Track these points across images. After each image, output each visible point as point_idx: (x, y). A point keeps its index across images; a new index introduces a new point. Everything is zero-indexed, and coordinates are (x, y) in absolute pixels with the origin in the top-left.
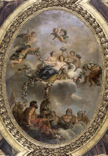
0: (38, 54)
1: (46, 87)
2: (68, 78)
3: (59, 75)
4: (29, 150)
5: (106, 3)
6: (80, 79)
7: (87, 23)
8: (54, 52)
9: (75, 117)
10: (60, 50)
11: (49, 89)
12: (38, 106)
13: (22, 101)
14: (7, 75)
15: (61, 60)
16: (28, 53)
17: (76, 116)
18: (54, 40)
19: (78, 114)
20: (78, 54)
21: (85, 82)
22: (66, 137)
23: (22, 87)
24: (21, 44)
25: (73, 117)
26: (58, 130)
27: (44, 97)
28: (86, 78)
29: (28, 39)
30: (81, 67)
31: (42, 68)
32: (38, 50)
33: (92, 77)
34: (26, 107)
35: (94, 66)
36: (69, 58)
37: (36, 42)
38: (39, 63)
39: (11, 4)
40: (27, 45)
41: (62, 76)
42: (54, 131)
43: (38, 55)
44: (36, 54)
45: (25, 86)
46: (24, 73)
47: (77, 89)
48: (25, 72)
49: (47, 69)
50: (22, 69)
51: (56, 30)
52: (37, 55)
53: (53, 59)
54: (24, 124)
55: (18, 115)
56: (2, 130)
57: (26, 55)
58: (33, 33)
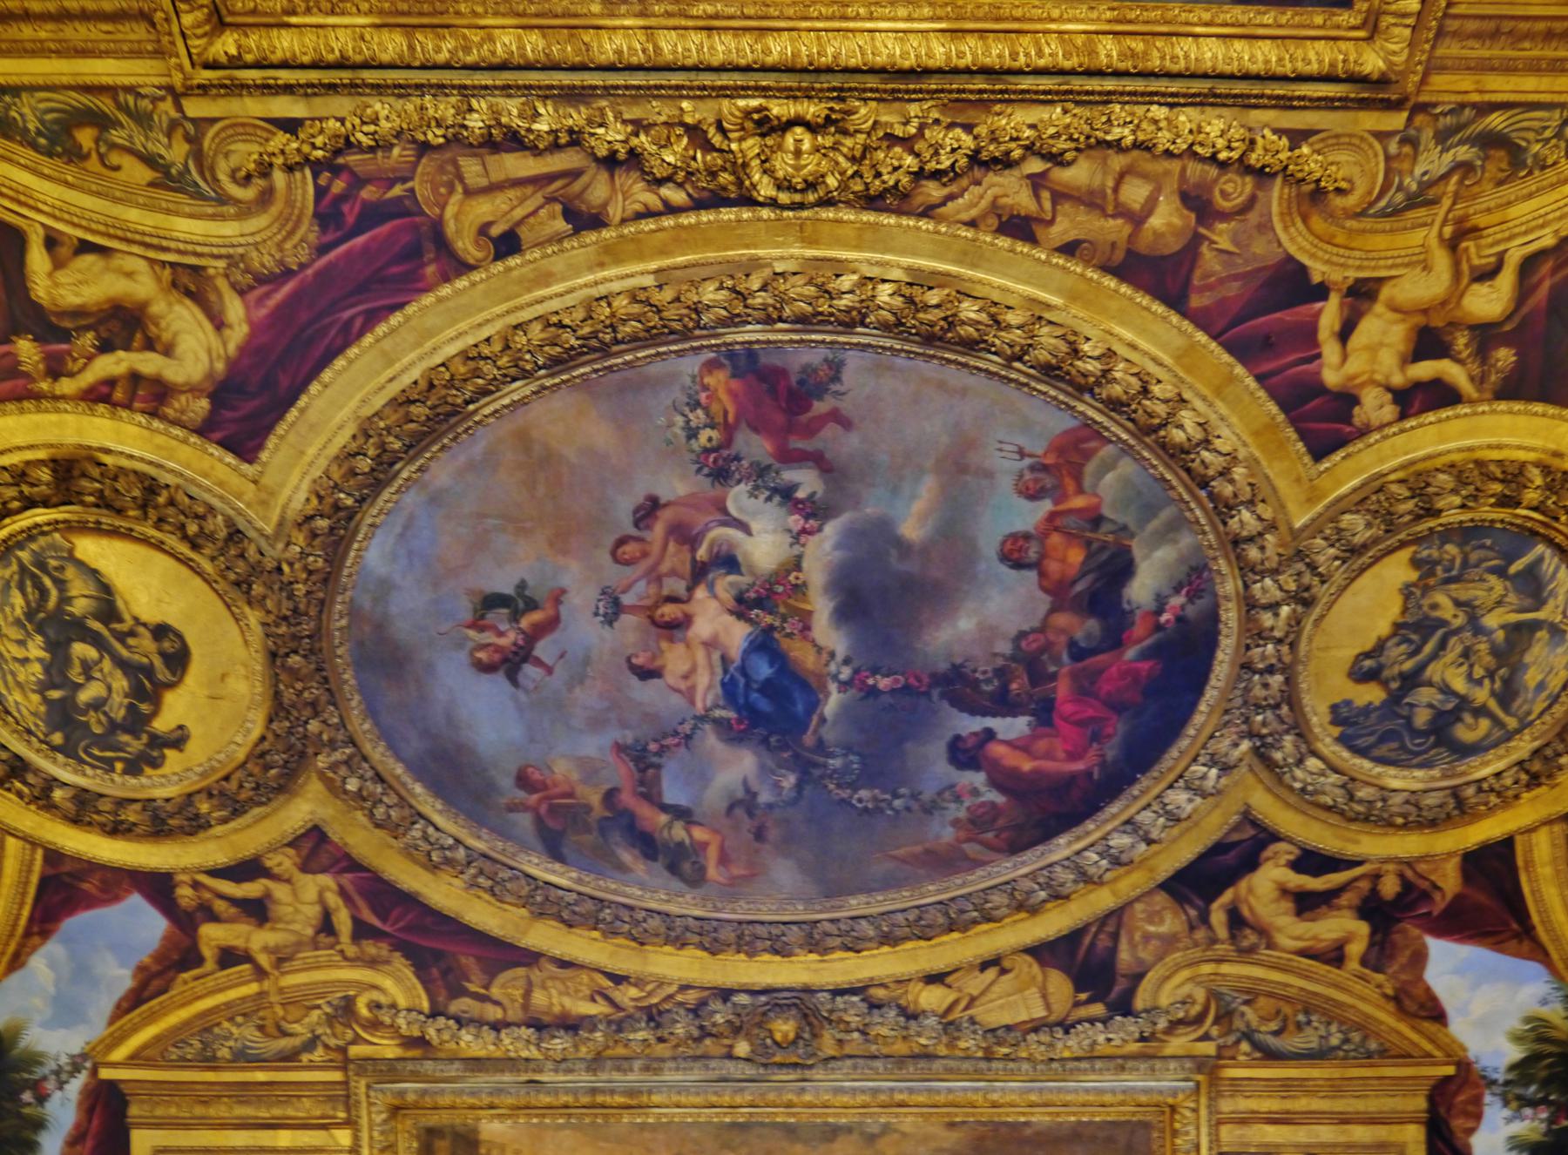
3: (777, 624)
5: (225, 344)
6: (801, 494)
7: (405, 474)
8: (634, 661)
9: (1052, 516)
10: (616, 624)
17: (1046, 506)
19: (1033, 495)
21: (818, 461)
22: (1182, 560)
25: (1056, 529)
26: (1132, 612)
27: (923, 701)
28: (789, 457)
30: (718, 490)
31: (739, 721)
33: (780, 419)
34: (983, 789)
35: (706, 410)
36: (665, 567)
38: (710, 740)
39: (361, 903)
41: (787, 605)
42: (1139, 629)
44: (655, 760)
45: (860, 800)
47: (868, 510)
48: (770, 806)
52: (659, 754)
53: (675, 660)
56: (1114, 893)
57: (665, 808)
58: (523, 780)
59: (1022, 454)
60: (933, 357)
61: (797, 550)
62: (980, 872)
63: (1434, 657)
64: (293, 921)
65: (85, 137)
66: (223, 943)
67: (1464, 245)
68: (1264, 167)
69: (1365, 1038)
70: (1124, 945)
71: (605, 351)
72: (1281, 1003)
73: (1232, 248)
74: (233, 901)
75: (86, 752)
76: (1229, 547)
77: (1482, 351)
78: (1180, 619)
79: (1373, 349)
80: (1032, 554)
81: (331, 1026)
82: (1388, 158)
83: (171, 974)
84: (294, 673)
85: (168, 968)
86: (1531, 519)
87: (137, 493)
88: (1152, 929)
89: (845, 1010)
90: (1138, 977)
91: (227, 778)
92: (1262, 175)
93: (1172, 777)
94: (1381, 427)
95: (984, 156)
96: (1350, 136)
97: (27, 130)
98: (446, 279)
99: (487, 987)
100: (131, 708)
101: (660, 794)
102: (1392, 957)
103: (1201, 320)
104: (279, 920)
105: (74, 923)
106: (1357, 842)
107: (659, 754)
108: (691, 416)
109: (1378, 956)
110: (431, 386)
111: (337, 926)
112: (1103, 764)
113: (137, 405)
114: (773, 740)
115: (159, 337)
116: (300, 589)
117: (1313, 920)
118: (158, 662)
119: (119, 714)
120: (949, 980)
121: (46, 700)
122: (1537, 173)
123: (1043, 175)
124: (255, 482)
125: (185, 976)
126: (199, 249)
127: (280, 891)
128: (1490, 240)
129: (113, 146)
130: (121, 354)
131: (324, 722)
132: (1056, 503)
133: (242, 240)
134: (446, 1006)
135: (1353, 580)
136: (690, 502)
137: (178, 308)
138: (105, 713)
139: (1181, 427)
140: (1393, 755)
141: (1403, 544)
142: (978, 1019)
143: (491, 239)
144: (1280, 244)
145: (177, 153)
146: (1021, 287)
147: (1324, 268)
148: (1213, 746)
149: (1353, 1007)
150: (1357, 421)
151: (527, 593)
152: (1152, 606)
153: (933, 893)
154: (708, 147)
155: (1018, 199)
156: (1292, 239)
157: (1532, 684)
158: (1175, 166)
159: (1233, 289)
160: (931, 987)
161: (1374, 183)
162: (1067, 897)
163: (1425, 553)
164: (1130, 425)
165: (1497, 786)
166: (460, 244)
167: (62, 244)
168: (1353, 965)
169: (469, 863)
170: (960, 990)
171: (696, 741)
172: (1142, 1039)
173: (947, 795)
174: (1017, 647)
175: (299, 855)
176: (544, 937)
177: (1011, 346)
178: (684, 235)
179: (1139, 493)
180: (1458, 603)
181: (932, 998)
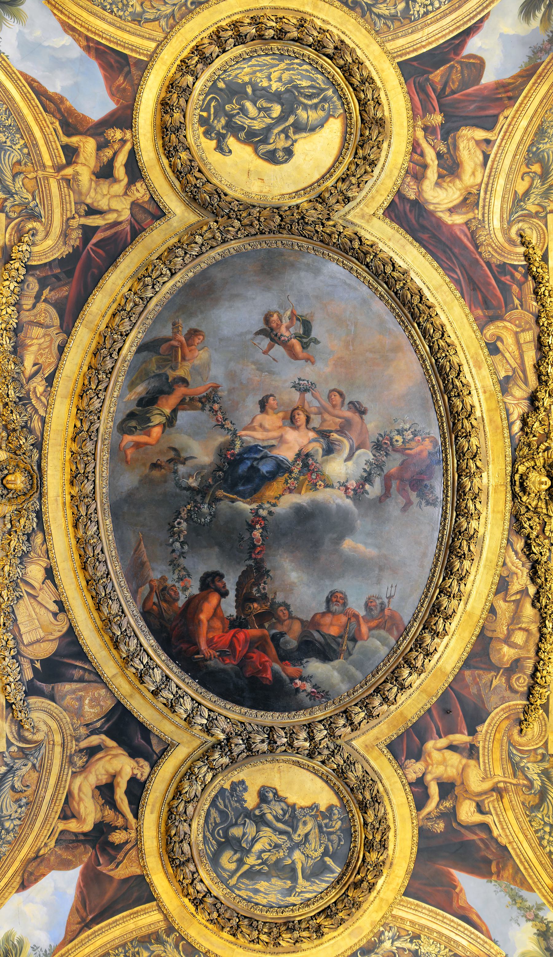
0: (216, 407)
1: (253, 521)
2: (327, 486)
3: (293, 475)
4: (209, 738)
6: (367, 487)
7: (380, 289)
8: (271, 398)
9: (356, 616)
11: (262, 528)
12: (228, 587)
14: (112, 485)
15: (299, 423)
16: (180, 407)
17: (362, 613)
18: (270, 353)
19: (367, 606)
20: (354, 398)
22: (332, 686)
23: (168, 527)
24: (155, 376)
25: (349, 619)
26: (302, 664)
27: (246, 556)
30: (370, 445)
31: (233, 455)
32: (216, 392)
33: (408, 475)
34: (187, 593)
36: (326, 416)
37: (207, 366)
38: (221, 438)
39: (109, 233)
40: (174, 379)
42: (291, 669)
43: (216, 411)
44: (208, 407)
45: (179, 523)
46: (173, 476)
48: (176, 472)
51: (272, 319)
52: (211, 409)
56: (114, 676)
57: (174, 411)
58: (193, 333)
59: (389, 598)
60: (440, 550)
62: (128, 595)
63: (275, 830)
64: (96, 193)
65: (536, 168)
67: (494, 794)
69: (9, 843)
70: (75, 686)
71: (446, 391)
72: (34, 788)
75: (213, 98)
76: (343, 709)
77: (442, 816)
78: (297, 690)
79: (444, 762)
81: (19, 205)
82: (535, 750)
83: (58, 116)
84: (272, 219)
85: (63, 115)
86: (358, 861)
87: (372, 157)
88: (87, 702)
89: (28, 519)
90: (52, 698)
91: (200, 171)
92: (530, 693)
93: (199, 699)
94: (404, 774)
95: (538, 567)
96: (546, 731)
97: (540, 143)
98: (476, 319)
99: (45, 301)
100: (242, 128)
101: (184, 409)
102: (67, 848)
103: (458, 678)
104: (97, 185)
105: (94, 68)
106: (152, 813)
107: (211, 409)
109: (68, 841)
110: (429, 308)
114: (220, 473)
116: (320, 228)
117: (93, 797)
118: (270, 147)
119: (238, 120)
120: (48, 581)
121: (247, 84)
122: (528, 819)
123: (528, 594)
124: (374, 214)
125: (57, 124)
126: (487, 208)
127: (119, 188)
129: (533, 179)
130: (436, 162)
131: (239, 229)
133: (491, 228)
134: (33, 275)
135: (321, 777)
136: (363, 431)
137: (458, 193)
138: (238, 113)
139: (410, 674)
140: (212, 820)
141: (341, 799)
142: (21, 601)
144: (495, 708)
145: (531, 206)
147: (484, 731)
148: (221, 719)
149: (32, 829)
150: (408, 761)
152: (305, 675)
153: (115, 568)
154: (539, 443)
156: (497, 713)
157: (257, 886)
158: (532, 654)
160: (43, 571)
162: (117, 648)
163: (336, 812)
164: (408, 649)
165: (195, 882)
168: (61, 826)
169: (142, 298)
170: (41, 589)
172: (9, 705)
174: (280, 605)
175: (144, 202)
176: (83, 338)
178: (499, 431)
179: (369, 659)
180: (307, 835)
181: (35, 572)
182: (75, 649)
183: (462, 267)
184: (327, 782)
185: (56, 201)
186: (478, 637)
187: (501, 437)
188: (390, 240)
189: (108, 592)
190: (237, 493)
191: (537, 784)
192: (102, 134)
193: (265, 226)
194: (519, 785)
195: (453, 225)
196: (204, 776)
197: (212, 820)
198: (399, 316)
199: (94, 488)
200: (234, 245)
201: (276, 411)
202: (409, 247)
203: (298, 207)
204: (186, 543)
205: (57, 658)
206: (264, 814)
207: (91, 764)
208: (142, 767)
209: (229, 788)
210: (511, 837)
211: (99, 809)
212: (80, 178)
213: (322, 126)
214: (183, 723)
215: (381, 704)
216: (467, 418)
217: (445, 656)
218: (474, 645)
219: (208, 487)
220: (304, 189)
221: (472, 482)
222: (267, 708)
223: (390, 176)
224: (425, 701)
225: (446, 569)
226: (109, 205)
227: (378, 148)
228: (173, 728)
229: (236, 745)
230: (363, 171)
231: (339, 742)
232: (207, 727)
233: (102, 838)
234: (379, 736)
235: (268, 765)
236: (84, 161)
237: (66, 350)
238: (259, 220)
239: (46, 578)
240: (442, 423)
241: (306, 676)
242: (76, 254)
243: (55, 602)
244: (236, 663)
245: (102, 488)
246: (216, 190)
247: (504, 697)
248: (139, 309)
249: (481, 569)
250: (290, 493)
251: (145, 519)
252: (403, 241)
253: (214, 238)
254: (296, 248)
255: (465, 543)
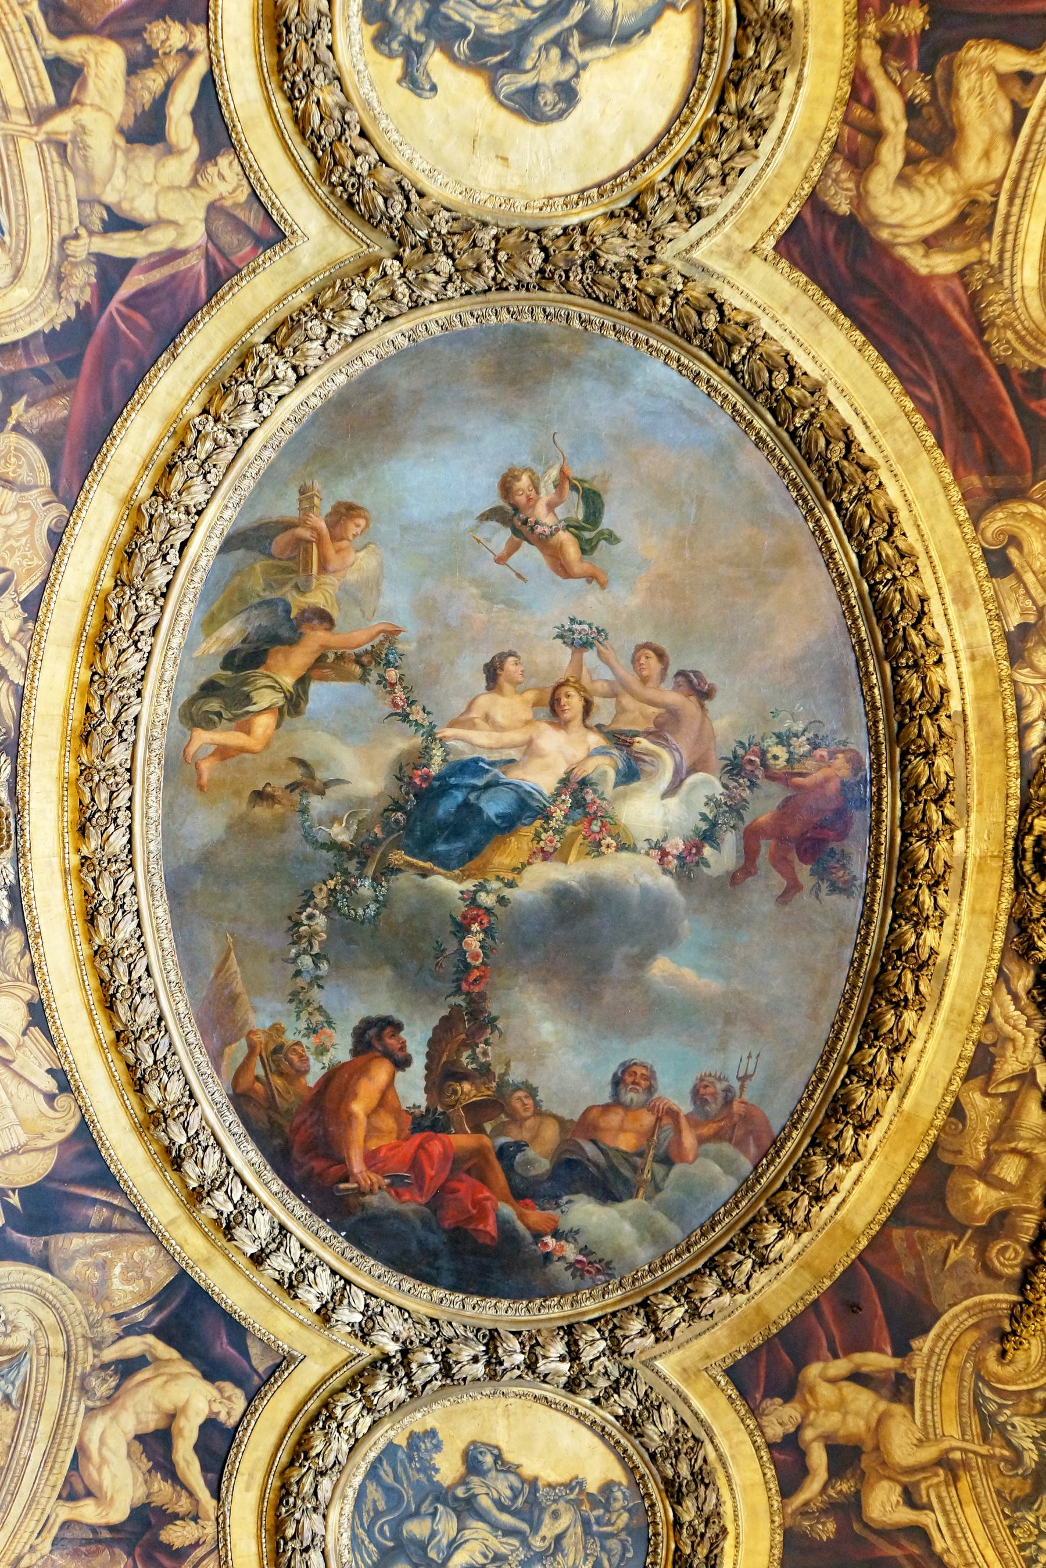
0: (392, 674)
1: (464, 917)
2: (621, 847)
3: (553, 824)
4: (366, 1350)
5: (907, 245)
6: (707, 851)
7: (758, 423)
8: (511, 659)
9: (673, 1114)
11: (485, 931)
12: (411, 1049)
13: (293, 1018)
14: (169, 837)
16: (316, 673)
17: (685, 1107)
18: (511, 561)
19: (698, 1095)
20: (688, 665)
21: (747, 867)
22: (619, 1251)
23: (288, 924)
24: (260, 604)
25: (659, 1119)
26: (558, 1206)
27: (451, 987)
28: (751, 838)
29: (308, 564)
31: (426, 778)
32: (392, 643)
33: (793, 830)
34: (326, 1059)
36: (627, 701)
37: (374, 584)
38: (402, 742)
39: (157, 276)
40: (304, 611)
42: (535, 1216)
43: (393, 685)
44: (374, 676)
45: (311, 917)
46: (298, 818)
48: (304, 811)
49: (466, 786)
50: (278, 793)
52: (382, 680)
54: (320, 1175)
55: (276, 1116)
56: (172, 1222)
57: (303, 682)
58: (345, 512)
60: (854, 986)
61: (642, 846)
62: (203, 1059)
63: (495, 1526)
64: (127, 178)
66: (91, 72)
67: (941, 1472)
68: (1031, 1283)
71: (890, 655)
73: (949, 1262)
74: (161, 102)
76: (639, 1300)
77: (832, 1509)
78: (547, 1257)
79: (841, 1405)
80: (628, 1096)
82: (1031, 1392)
87: (758, 111)
88: (117, 1270)
90: (45, 1265)
91: (363, 134)
92: (1025, 1281)
93: (347, 1272)
94: (760, 1427)
98: (965, 496)
99: (17, 428)
100: (462, 31)
103: (879, 1242)
104: (129, 159)
106: (247, 1489)
107: (382, 680)
108: (803, 739)
110: (865, 470)
111: (118, 236)
112: (360, 1192)
113: (847, 130)
115: (919, 172)
116: (631, 281)
117: (129, 1456)
118: (526, 80)
120: (35, 1031)
122: (1006, 1523)
126: (1010, 237)
128: (944, 1494)
130: (904, 126)
131: (450, 279)
132: (687, 1116)
133: (1017, 286)
136: (704, 735)
137: (948, 201)
139: (781, 1236)
143: (1005, 548)
144: (951, 1306)
146: (922, 1068)
147: (925, 1350)
148: (391, 1312)
150: (768, 1401)
151: (603, 543)
152: (564, 1225)
155: (1011, 1060)
156: (956, 1316)
159: (909, 1268)
160: (24, 1010)
161: (1007, 1383)
163: (619, 1495)
166: (1000, 515)
167: (1023, 90)
168: (65, 1512)
169: (232, 433)
170: (19, 1046)
171: (397, 723)
173: (318, 1018)
174: (518, 1088)
175: (236, 205)
177: (870, 1064)
180: (559, 1538)
182: (93, 1167)
183: (944, 377)
184: (603, 1434)
185: (35, 192)
186: (924, 1163)
187: (1001, 755)
188: (786, 310)
189: (160, 1056)
190: (430, 858)
191: (1031, 1457)
192: (137, 34)
193: (508, 272)
194: (993, 1456)
195: (931, 277)
196: (356, 1422)
197: (370, 1505)
198: (795, 485)
199: (130, 841)
200: (436, 314)
201: (519, 688)
202: (828, 328)
203: (583, 228)
204: (325, 957)
205: (54, 1185)
206: (475, 1496)
207: (127, 1391)
208: (229, 1399)
209: (404, 1444)
210: (969, 1555)
211: (141, 1478)
212: (89, 140)
213: (647, 30)
214: (312, 1319)
215: (719, 1293)
216: (930, 715)
217: (852, 1198)
218: (916, 1178)
219: (372, 844)
220: (599, 186)
221: (931, 852)
222: (485, 1291)
223: (794, 158)
224: (807, 1286)
225: (865, 1025)
226: (156, 209)
227: (774, 88)
228: (293, 1326)
229: (420, 1365)
230: (735, 144)
231: (628, 1363)
232: (362, 1330)
233: (147, 1536)
234: (711, 1352)
235: (483, 1402)
236: (97, 101)
237: (65, 541)
238: (494, 258)
239: (30, 1024)
240: (876, 723)
241: (567, 1229)
242: (84, 321)
243: (50, 1071)
244: (424, 1200)
245: (146, 841)
246: (399, 183)
247: (970, 1285)
248: (226, 455)
249: (938, 1028)
250: (545, 859)
251: (239, 907)
252: (816, 314)
253: (393, 296)
254: (576, 324)
255: (909, 975)
